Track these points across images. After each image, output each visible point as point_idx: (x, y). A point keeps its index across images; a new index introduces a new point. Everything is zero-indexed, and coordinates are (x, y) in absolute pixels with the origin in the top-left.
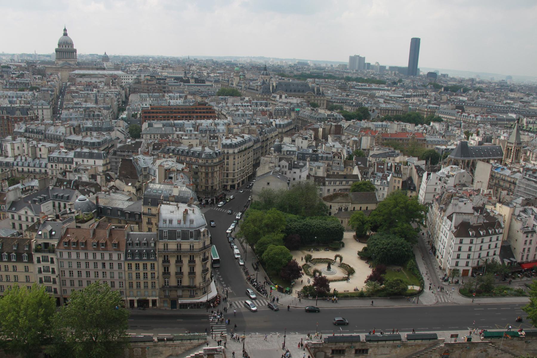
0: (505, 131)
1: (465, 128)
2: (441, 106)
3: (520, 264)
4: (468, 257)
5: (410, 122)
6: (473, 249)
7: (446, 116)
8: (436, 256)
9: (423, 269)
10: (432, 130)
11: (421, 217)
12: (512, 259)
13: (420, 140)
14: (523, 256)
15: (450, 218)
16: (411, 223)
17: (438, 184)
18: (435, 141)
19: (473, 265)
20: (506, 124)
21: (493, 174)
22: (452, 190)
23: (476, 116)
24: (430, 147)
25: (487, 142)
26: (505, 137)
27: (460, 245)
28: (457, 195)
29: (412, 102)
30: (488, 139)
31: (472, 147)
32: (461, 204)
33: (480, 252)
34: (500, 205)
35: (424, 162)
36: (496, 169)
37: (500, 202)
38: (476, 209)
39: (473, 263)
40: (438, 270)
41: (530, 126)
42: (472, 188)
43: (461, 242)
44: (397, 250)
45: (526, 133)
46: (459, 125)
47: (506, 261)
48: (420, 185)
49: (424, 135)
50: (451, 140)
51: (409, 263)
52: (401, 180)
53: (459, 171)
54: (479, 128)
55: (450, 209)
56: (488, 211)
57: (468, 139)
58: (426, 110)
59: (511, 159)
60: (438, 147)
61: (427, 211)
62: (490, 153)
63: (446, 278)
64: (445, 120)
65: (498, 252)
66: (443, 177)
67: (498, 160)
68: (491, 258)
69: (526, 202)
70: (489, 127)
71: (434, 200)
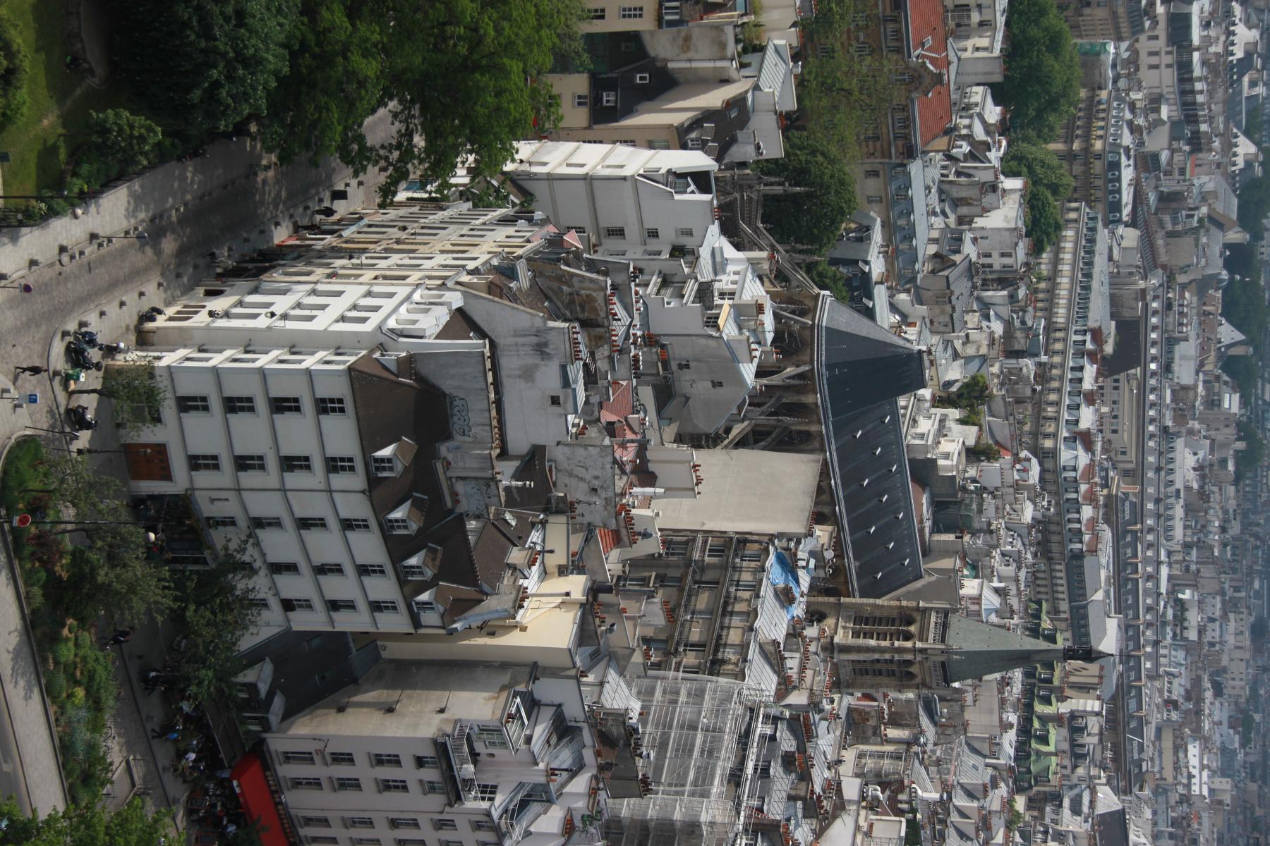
0: (1014, 602)
1: (1009, 379)
2: (1131, 237)
3: (258, 753)
4: (244, 463)
5: (1015, 48)
6: (295, 479)
7: (1066, 268)
8: (216, 286)
9: (113, 212)
10: (972, 193)
11: (441, 165)
12: (278, 703)
13: (907, 122)
14: (307, 758)
15: (463, 321)
16: (393, 105)
17: (653, 245)
18: (910, 211)
19: (202, 499)
20: (1055, 611)
21: (752, 549)
22: (622, 323)
23: (1086, 439)
24: (872, 186)
25: (938, 506)
26: (977, 600)
27: (307, 405)
28: (604, 351)
29: (1145, 60)
30: (953, 509)
31: (896, 421)
32: (549, 378)
33: (288, 522)
34: (578, 594)
35: (774, 147)
36: (781, 560)
37: (595, 590)
38: (534, 462)
39: (212, 492)
40: (135, 306)
41: (1056, 736)
42: (653, 437)
43: (325, 406)
44: (206, 32)
45: (1013, 718)
46: (1020, 342)
47: (261, 676)
48: (632, 143)
49: (942, 143)
50: (923, 310)
51: (140, 120)
52: (643, 25)
53: (742, 352)
54: (1017, 460)
55: (512, 320)
56: (535, 536)
57: (941, 401)
58: (1098, 145)
59: (850, 641)
60: (877, 236)
61: (478, 198)
62: (878, 532)
63: (94, 354)
64: (1044, 269)
65: (303, 622)
66: (694, 264)
67: (839, 571)
68: (260, 584)
69: (615, 731)
70: (1028, 513)
71: (551, 229)
